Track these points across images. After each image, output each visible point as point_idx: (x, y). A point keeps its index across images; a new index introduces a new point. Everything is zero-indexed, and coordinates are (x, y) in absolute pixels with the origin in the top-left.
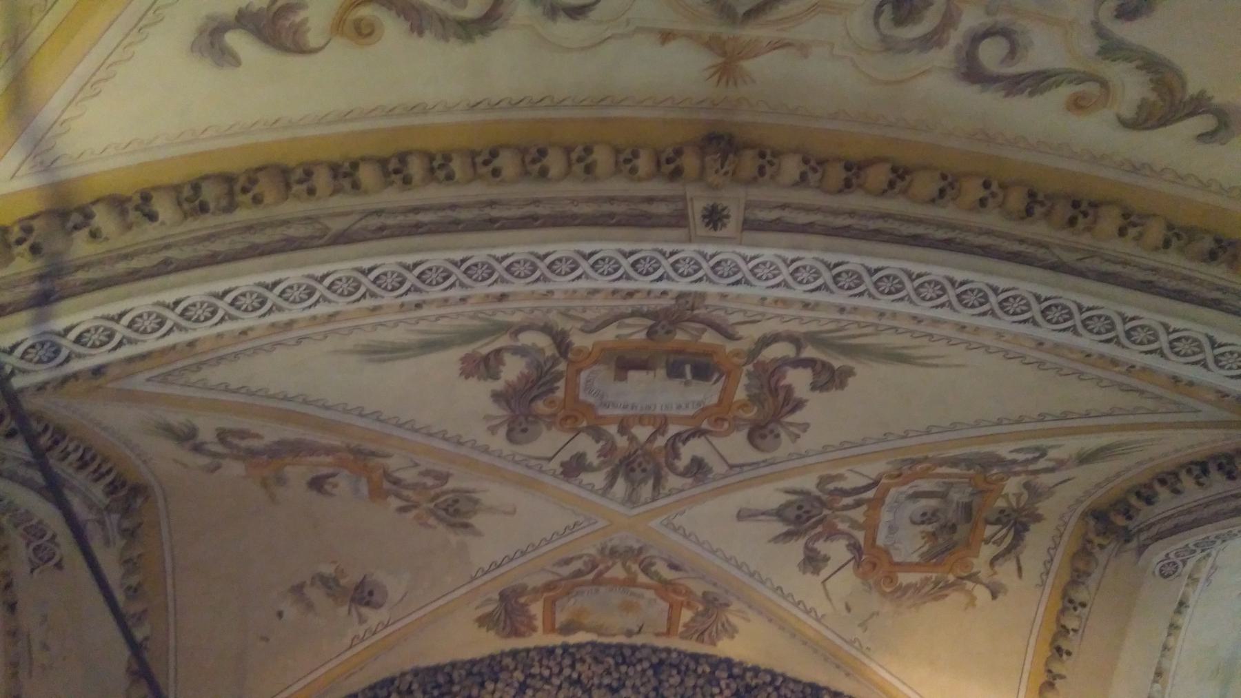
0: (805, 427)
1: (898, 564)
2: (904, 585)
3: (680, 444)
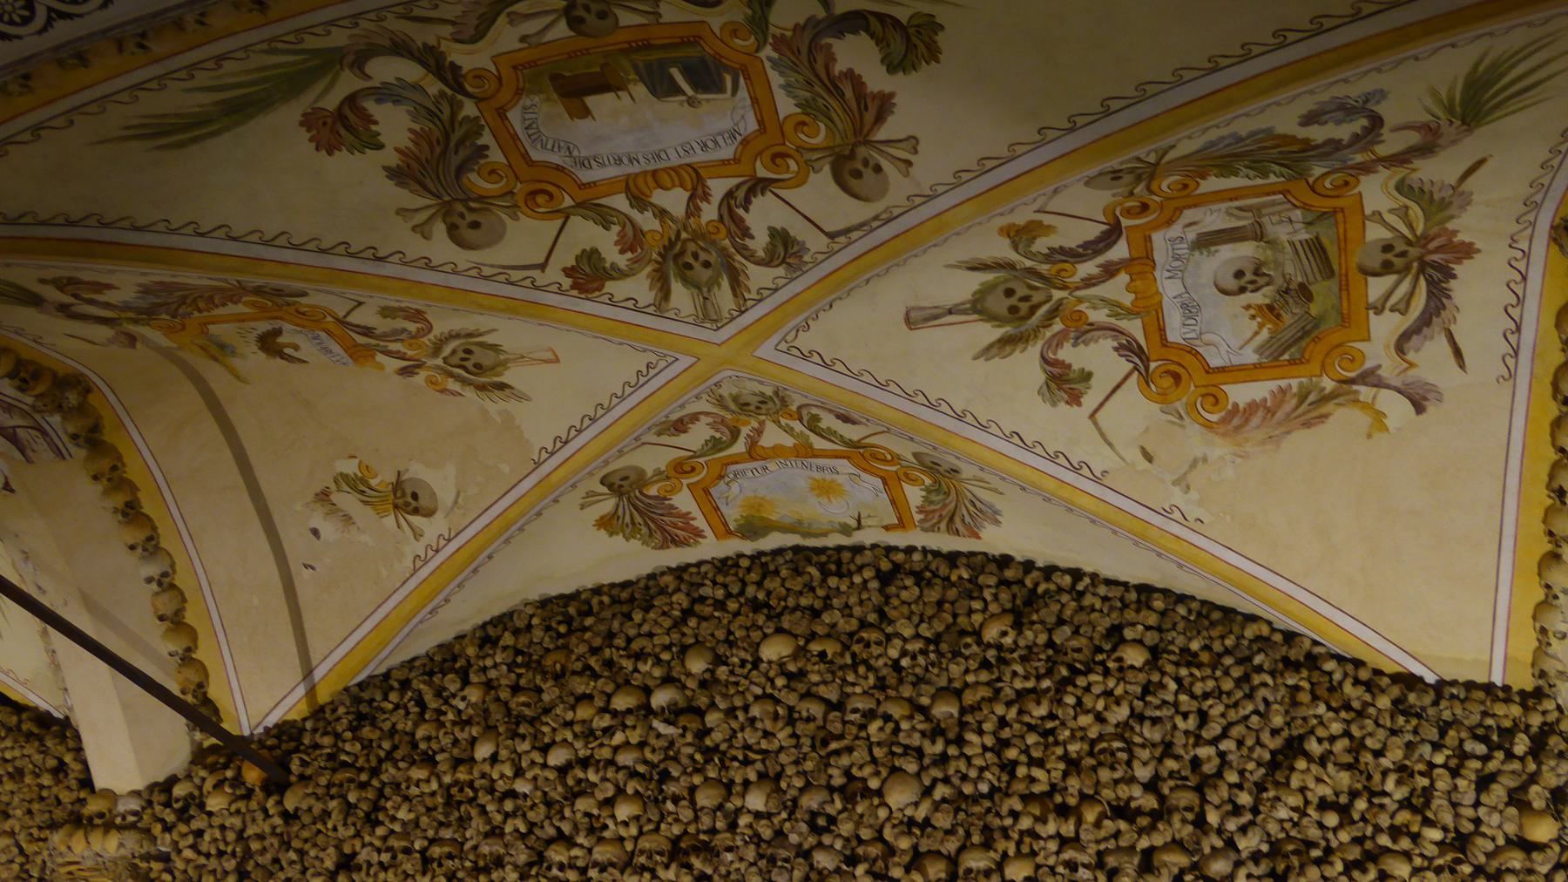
0: (913, 142)
1: (1222, 370)
2: (1242, 406)
3: (741, 212)
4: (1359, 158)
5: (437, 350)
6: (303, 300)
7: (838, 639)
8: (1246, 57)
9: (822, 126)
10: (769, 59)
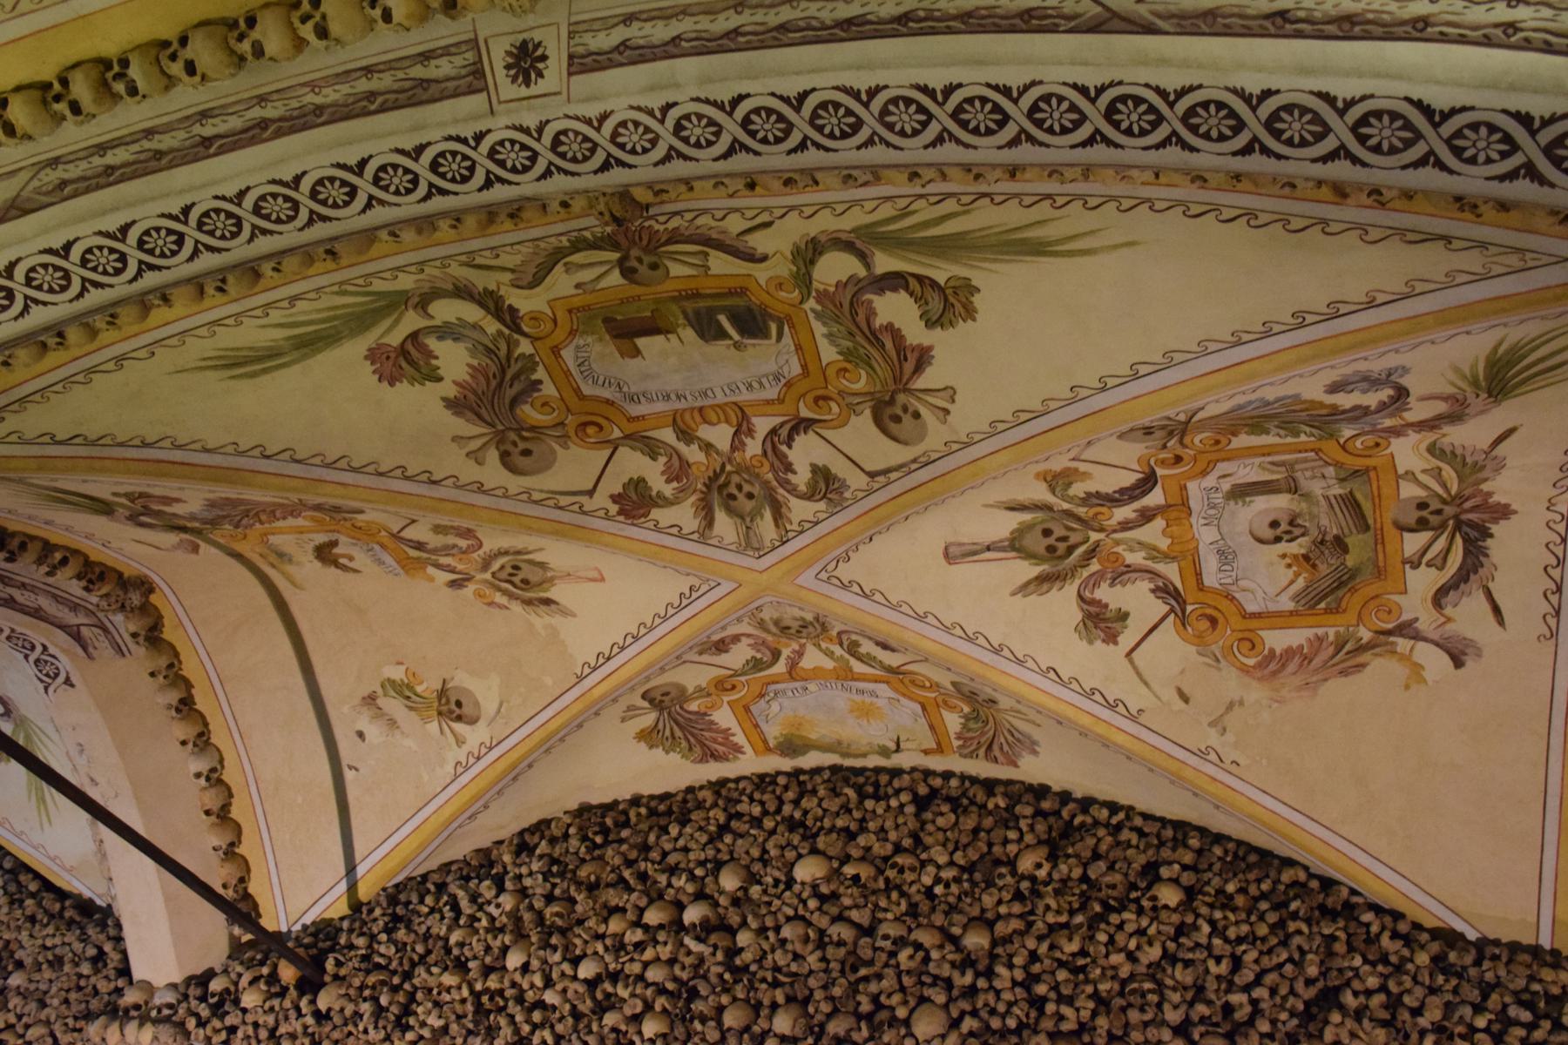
0: (951, 392)
1: (1255, 616)
2: (1278, 652)
3: (784, 448)
4: (1388, 423)
5: (485, 566)
6: (359, 517)
7: (872, 863)
8: (1268, 334)
9: (863, 373)
10: (813, 310)
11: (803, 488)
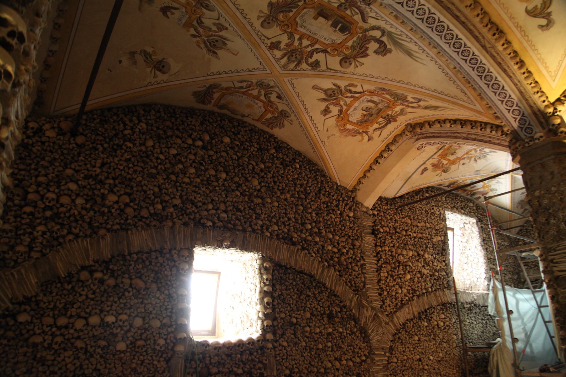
0: (362, 64)
3: (315, 53)
11: (309, 62)
